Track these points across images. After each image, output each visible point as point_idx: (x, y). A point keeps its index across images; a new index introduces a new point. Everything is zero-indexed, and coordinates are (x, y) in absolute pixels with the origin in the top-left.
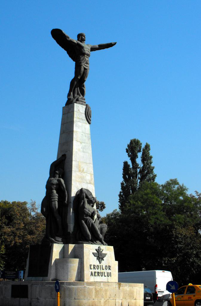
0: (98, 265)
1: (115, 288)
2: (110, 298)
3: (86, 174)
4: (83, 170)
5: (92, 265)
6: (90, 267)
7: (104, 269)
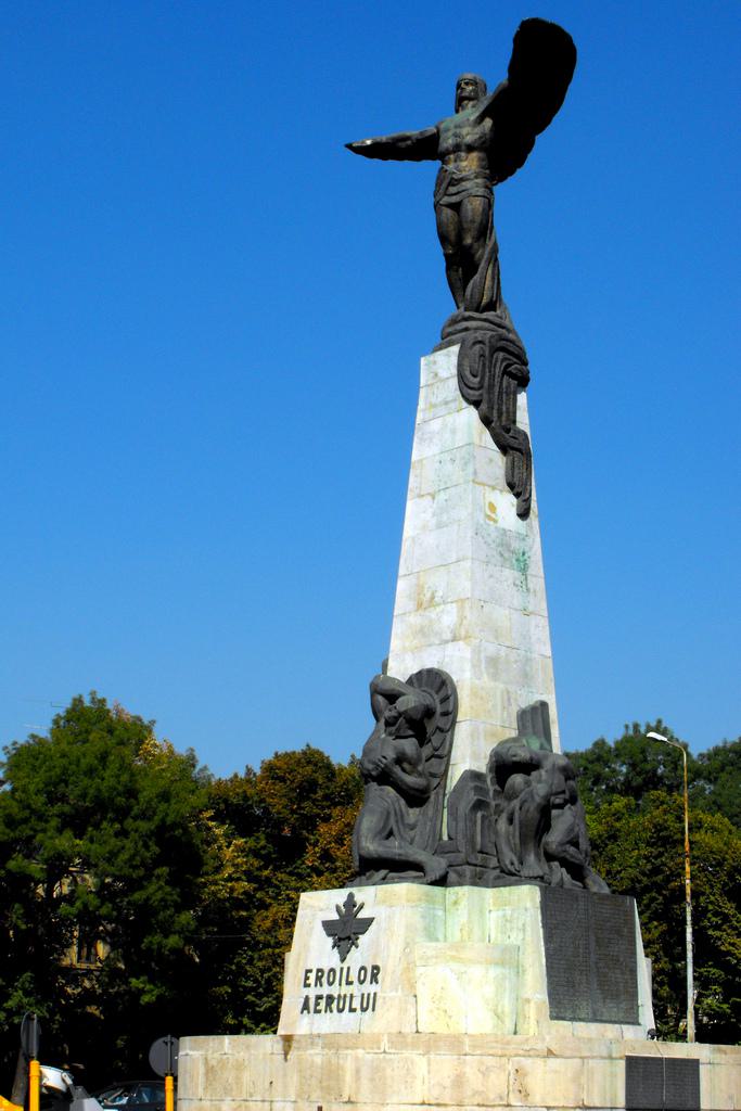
0: (334, 966)
1: (272, 1054)
2: (251, 1096)
3: (443, 606)
4: (433, 598)
5: (310, 971)
6: (307, 978)
7: (351, 983)
